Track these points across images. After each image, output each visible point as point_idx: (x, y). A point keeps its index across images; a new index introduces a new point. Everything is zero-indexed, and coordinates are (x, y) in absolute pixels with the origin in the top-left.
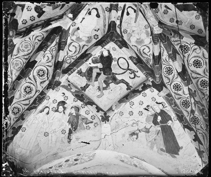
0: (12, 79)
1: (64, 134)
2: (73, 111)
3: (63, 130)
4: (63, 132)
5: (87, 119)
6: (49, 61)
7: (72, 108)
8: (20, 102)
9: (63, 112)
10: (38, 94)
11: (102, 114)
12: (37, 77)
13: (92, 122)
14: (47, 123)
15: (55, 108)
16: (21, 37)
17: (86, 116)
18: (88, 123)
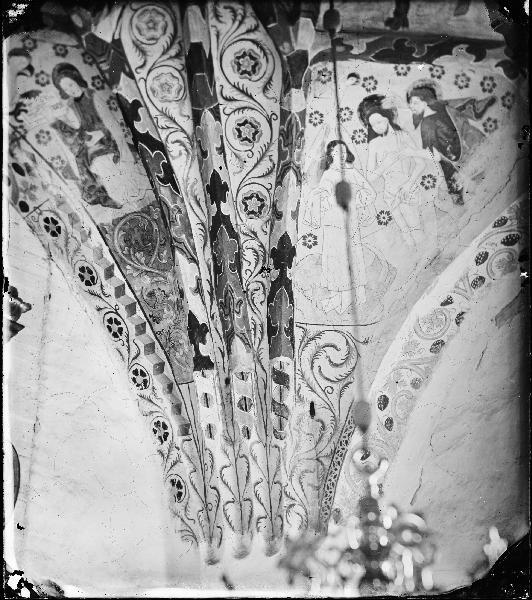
0: (183, 131)
1: (434, 186)
2: (421, 106)
3: (424, 178)
4: (427, 182)
5: (472, 101)
6: (239, 18)
7: (408, 99)
8: (250, 176)
9: (390, 127)
10: (276, 124)
11: (496, 57)
12: (244, 83)
13: (492, 101)
14: (366, 185)
15: (362, 131)
16: (105, 10)
17: (466, 94)
18: (484, 111)
